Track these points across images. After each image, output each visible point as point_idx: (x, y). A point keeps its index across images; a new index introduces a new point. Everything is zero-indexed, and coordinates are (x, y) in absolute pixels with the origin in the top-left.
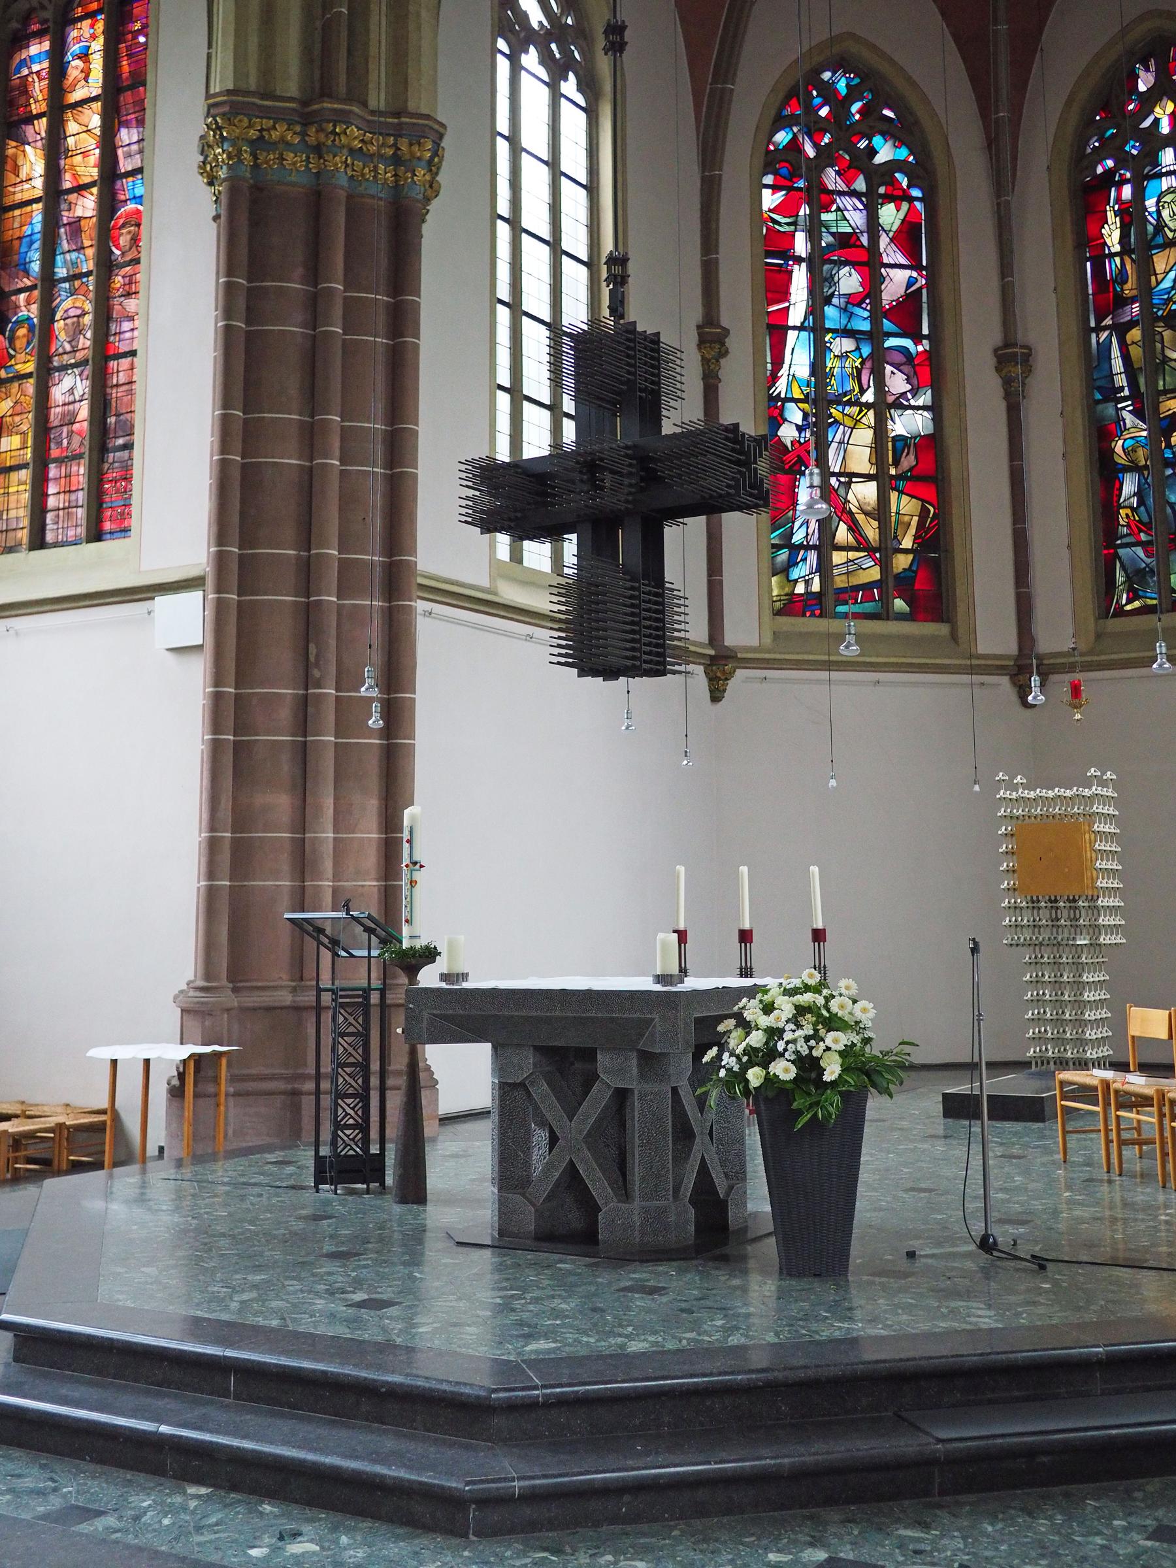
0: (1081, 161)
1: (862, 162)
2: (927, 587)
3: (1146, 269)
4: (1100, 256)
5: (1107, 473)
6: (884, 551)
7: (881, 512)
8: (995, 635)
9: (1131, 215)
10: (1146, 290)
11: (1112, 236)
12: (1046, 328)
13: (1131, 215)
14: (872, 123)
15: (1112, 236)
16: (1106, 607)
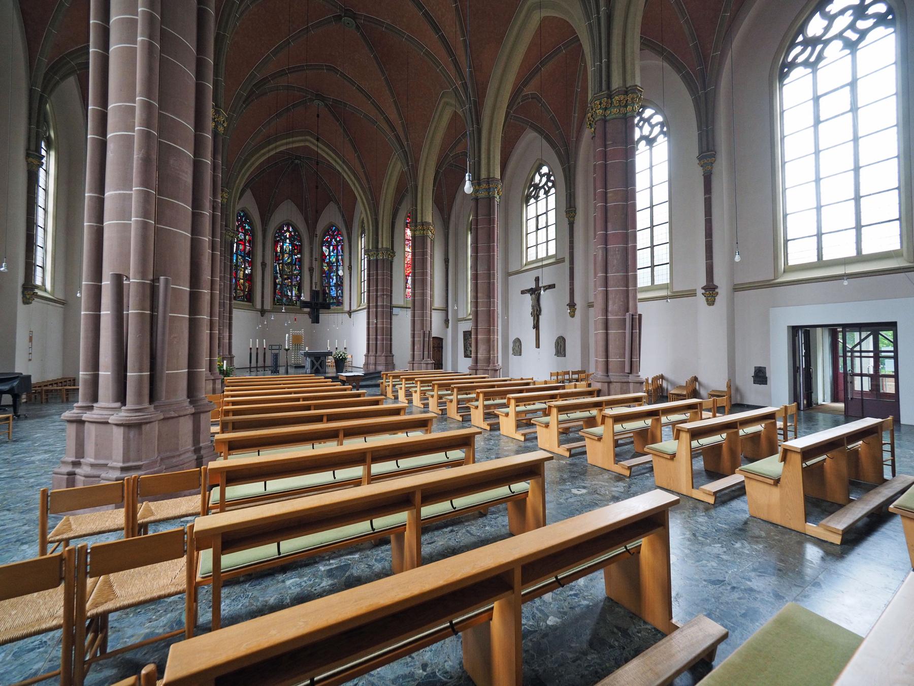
0: (276, 237)
1: (244, 228)
2: (249, 298)
3: (283, 256)
4: (277, 252)
5: (275, 284)
6: (243, 291)
7: (244, 285)
8: (259, 306)
9: (282, 247)
10: (283, 259)
11: (279, 249)
12: (269, 261)
13: (282, 247)
14: (245, 222)
15: (279, 249)
16: (274, 304)
